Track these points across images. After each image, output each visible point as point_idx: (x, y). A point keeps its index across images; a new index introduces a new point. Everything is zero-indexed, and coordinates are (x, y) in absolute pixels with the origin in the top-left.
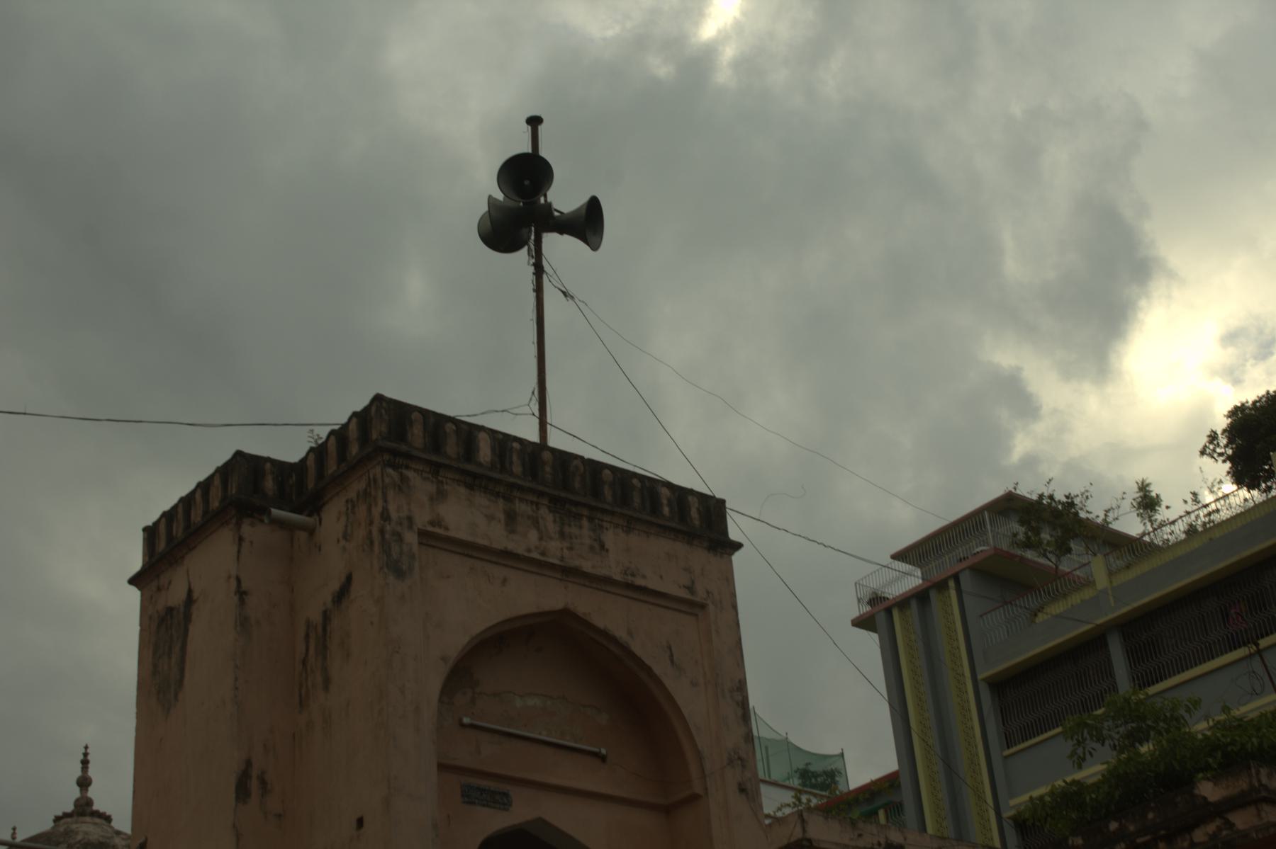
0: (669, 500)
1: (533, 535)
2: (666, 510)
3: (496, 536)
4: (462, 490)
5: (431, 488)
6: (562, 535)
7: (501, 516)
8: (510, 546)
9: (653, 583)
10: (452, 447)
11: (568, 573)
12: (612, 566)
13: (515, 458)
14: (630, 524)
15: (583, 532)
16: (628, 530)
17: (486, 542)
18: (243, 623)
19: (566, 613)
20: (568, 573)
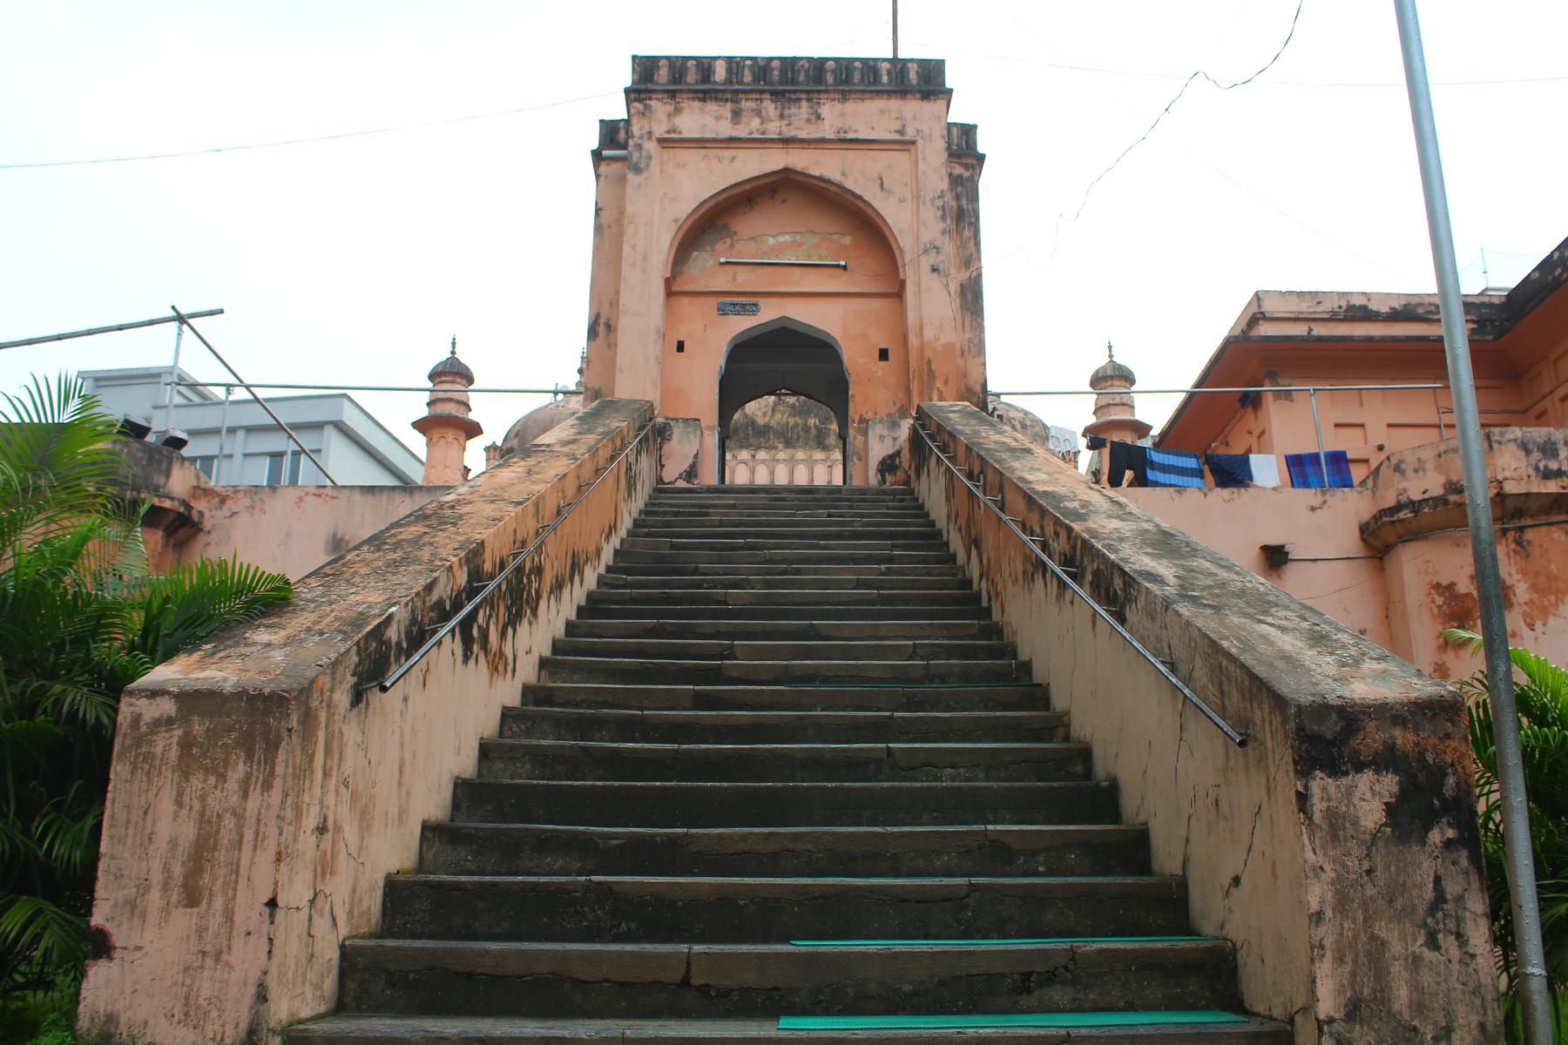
0: (889, 72)
1: (756, 123)
2: (885, 79)
3: (726, 129)
4: (696, 104)
5: (670, 108)
6: (782, 116)
7: (729, 115)
8: (734, 134)
9: (863, 135)
10: (692, 77)
11: (787, 142)
12: (827, 130)
13: (746, 72)
14: (845, 96)
15: (804, 110)
16: (845, 100)
17: (713, 136)
18: (598, 228)
19: (786, 170)
20: (787, 142)
